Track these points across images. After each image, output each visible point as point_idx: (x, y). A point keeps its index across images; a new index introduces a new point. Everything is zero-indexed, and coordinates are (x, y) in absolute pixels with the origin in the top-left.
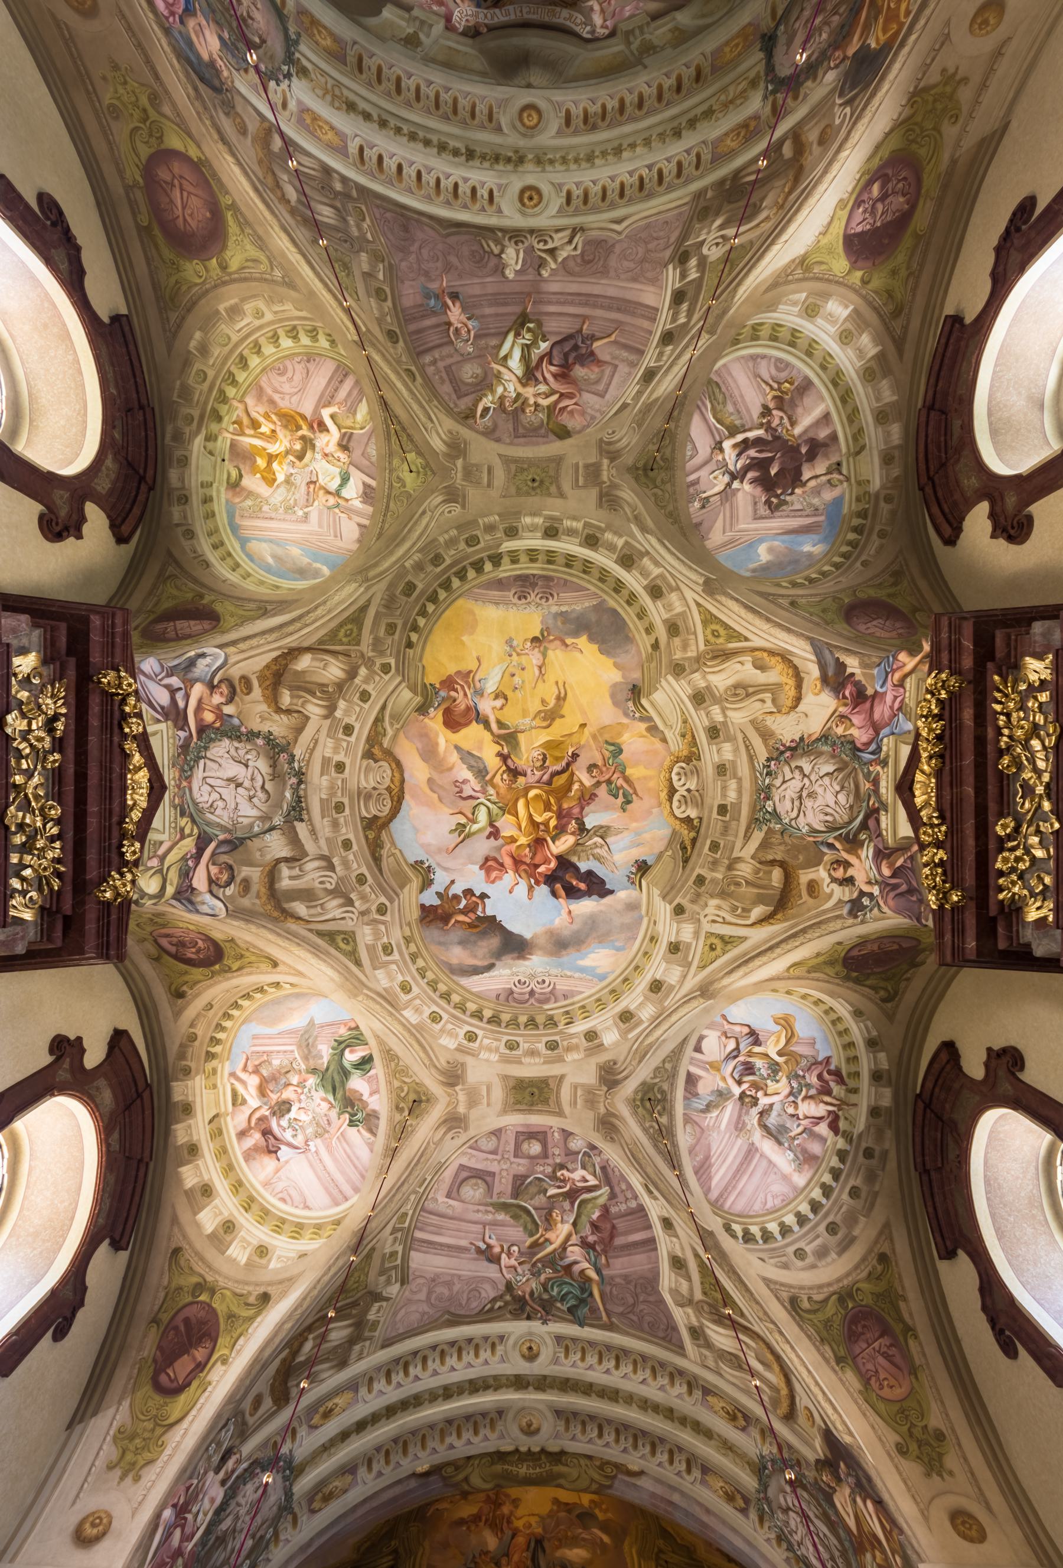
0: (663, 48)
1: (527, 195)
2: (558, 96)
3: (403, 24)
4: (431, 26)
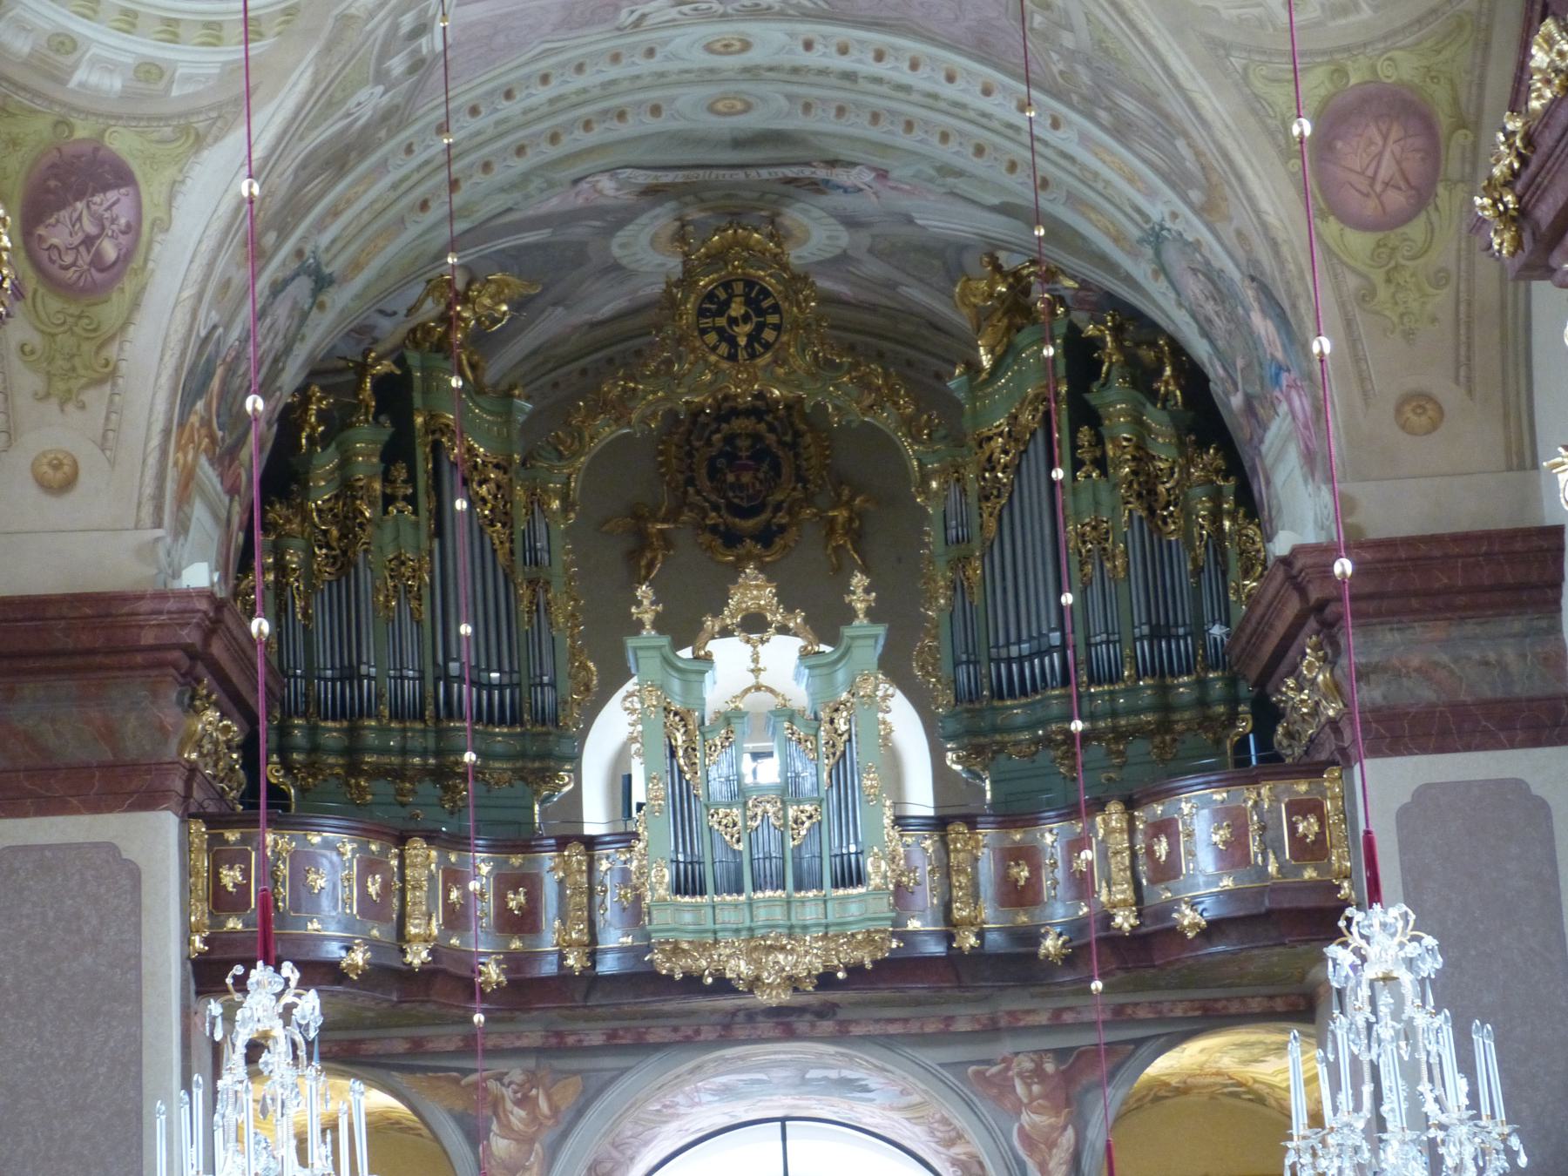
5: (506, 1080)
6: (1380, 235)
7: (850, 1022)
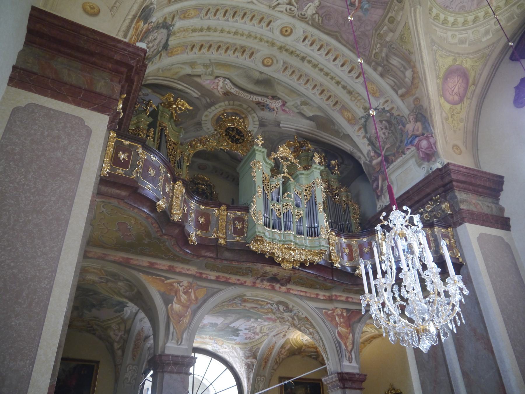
0: (200, 64)
1: (288, 33)
2: (252, 65)
3: (305, 110)
4: (293, 105)
5: (181, 284)
6: (452, 105)
7: (291, 289)
